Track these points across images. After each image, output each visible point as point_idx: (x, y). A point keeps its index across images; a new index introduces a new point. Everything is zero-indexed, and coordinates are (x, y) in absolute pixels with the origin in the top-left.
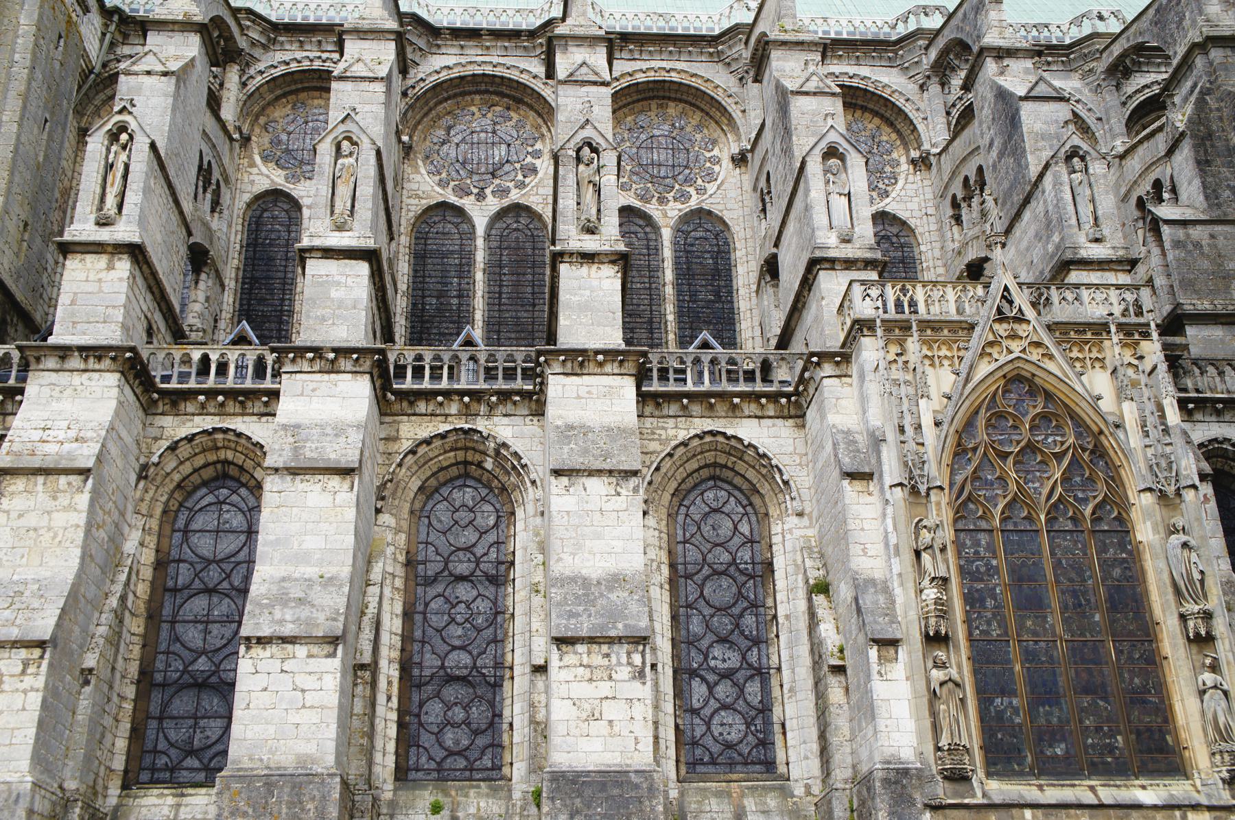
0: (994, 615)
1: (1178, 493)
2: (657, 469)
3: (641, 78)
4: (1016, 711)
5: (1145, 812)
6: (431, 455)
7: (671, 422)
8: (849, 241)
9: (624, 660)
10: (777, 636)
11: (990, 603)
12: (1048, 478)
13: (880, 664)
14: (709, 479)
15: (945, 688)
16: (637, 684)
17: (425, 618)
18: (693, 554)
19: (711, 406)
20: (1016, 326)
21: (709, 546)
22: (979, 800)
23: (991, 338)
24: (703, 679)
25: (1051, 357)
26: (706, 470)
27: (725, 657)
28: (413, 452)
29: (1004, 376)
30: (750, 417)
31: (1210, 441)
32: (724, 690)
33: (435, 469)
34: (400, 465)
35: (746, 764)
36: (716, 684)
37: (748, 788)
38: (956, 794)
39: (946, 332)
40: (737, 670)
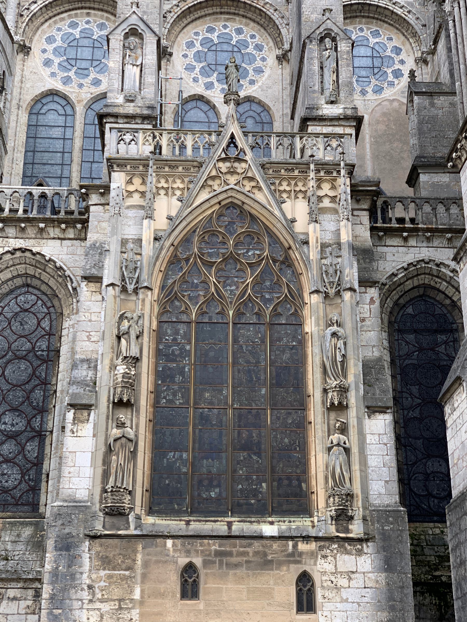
0: (180, 388)
1: (338, 294)
4: (184, 463)
5: (264, 542)
8: (132, 101)
10: (54, 407)
11: (178, 378)
12: (243, 283)
13: (74, 424)
15: (118, 443)
19: (23, 229)
20: (236, 165)
22: (132, 531)
23: (214, 173)
25: (260, 189)
26: (19, 279)
29: (219, 203)
30: (54, 238)
31: (418, 262)
35: (17, 504)
37: (10, 523)
38: (113, 527)
39: (180, 168)
40: (22, 432)
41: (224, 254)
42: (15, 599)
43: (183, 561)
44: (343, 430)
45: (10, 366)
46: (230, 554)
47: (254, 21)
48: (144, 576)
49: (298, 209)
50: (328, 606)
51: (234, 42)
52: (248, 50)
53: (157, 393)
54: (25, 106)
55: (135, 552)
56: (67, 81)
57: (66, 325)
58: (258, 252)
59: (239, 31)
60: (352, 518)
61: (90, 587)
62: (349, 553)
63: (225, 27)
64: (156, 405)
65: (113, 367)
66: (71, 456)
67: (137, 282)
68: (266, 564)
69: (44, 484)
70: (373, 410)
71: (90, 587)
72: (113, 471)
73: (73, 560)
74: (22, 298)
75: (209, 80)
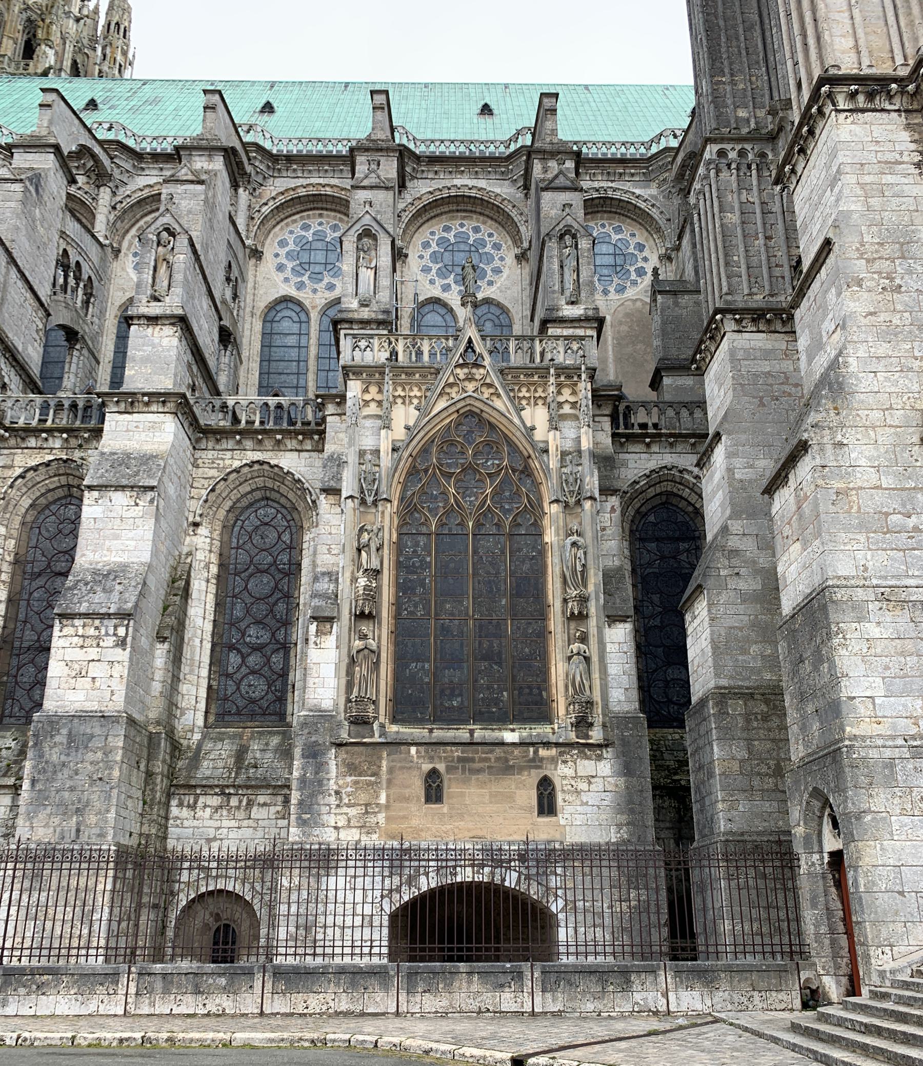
1: (578, 503)
2: (213, 490)
3: (302, 192)
5: (506, 748)
6: (38, 479)
7: (229, 454)
9: (111, 631)
11: (419, 590)
13: (317, 636)
14: (263, 499)
15: (361, 654)
16: (119, 650)
17: (28, 604)
18: (243, 557)
19: (260, 441)
21: (257, 551)
22: (377, 739)
24: (239, 651)
25: (499, 396)
27: (255, 635)
28: (22, 476)
29: (457, 411)
31: (661, 468)
32: (254, 660)
33: (43, 491)
34: (11, 487)
36: (249, 655)
41: (462, 465)
42: (265, 804)
43: (427, 767)
44: (584, 639)
45: (252, 580)
46: (472, 760)
47: (492, 219)
48: (389, 782)
49: (537, 416)
50: (569, 809)
51: (471, 242)
52: (486, 250)
53: (398, 605)
54: (258, 314)
55: (380, 758)
56: (300, 286)
57: (306, 538)
58: (497, 462)
59: (476, 230)
60: (591, 724)
61: (337, 793)
62: (588, 758)
63: (462, 225)
64: (397, 616)
65: (354, 580)
66: (314, 667)
67: (376, 494)
68: (506, 769)
69: (290, 694)
70: (612, 619)
71: (337, 793)
72: (357, 681)
73: (320, 767)
74: (261, 511)
75: (446, 282)
